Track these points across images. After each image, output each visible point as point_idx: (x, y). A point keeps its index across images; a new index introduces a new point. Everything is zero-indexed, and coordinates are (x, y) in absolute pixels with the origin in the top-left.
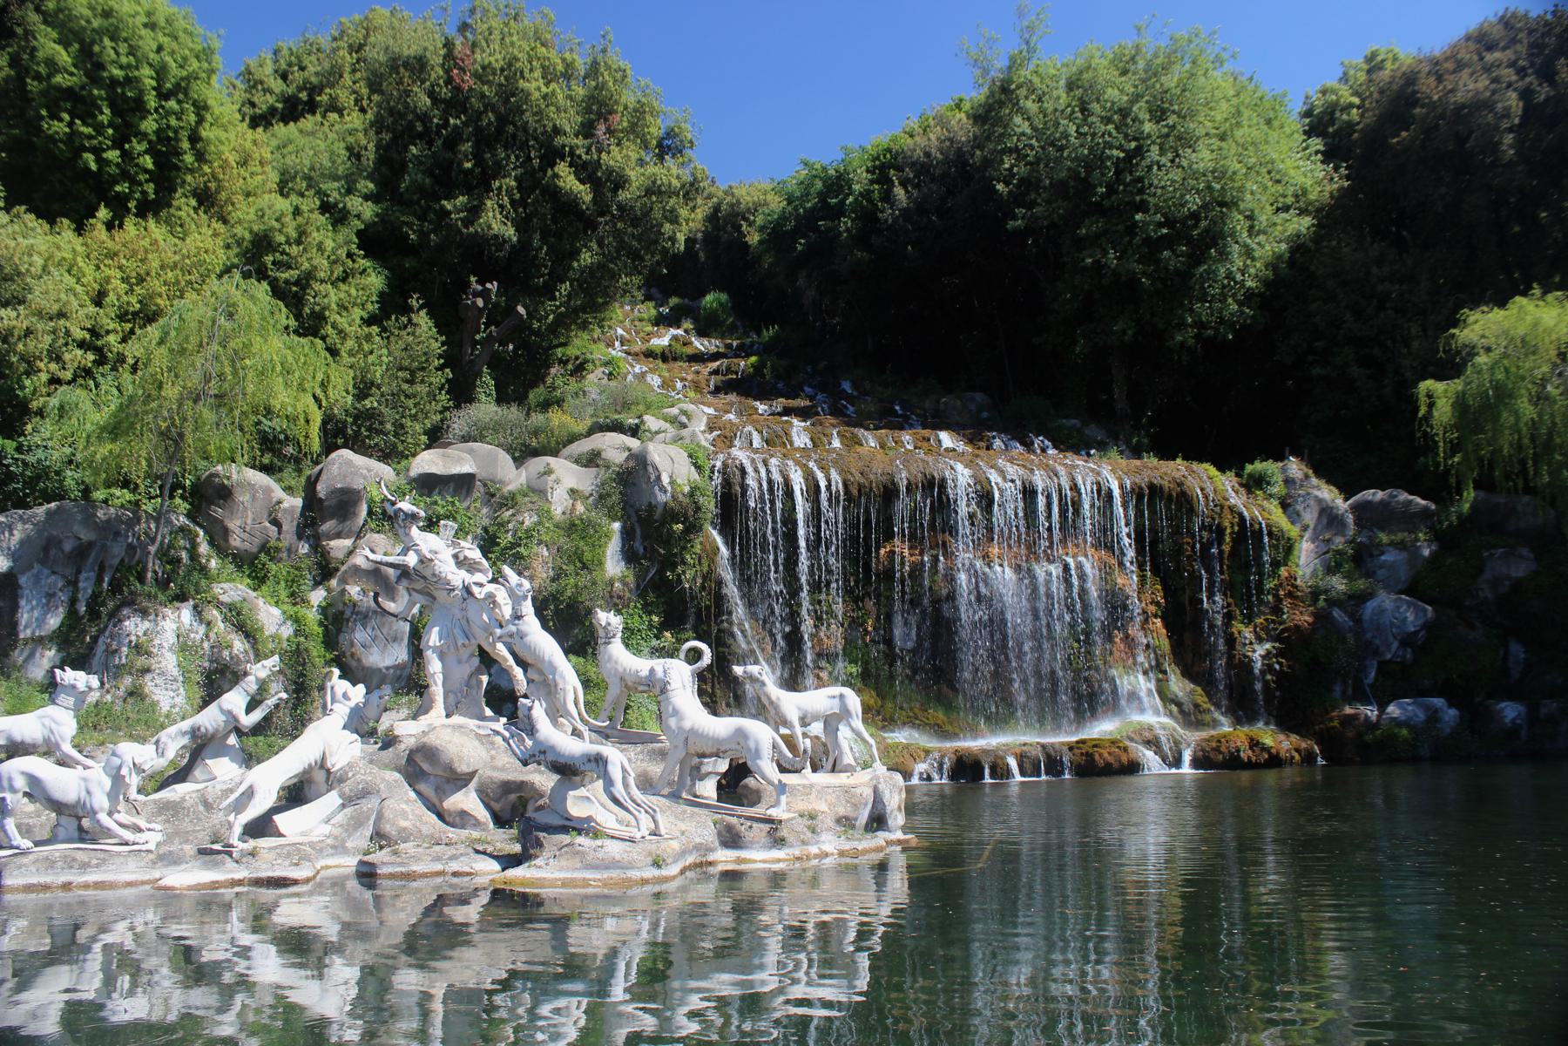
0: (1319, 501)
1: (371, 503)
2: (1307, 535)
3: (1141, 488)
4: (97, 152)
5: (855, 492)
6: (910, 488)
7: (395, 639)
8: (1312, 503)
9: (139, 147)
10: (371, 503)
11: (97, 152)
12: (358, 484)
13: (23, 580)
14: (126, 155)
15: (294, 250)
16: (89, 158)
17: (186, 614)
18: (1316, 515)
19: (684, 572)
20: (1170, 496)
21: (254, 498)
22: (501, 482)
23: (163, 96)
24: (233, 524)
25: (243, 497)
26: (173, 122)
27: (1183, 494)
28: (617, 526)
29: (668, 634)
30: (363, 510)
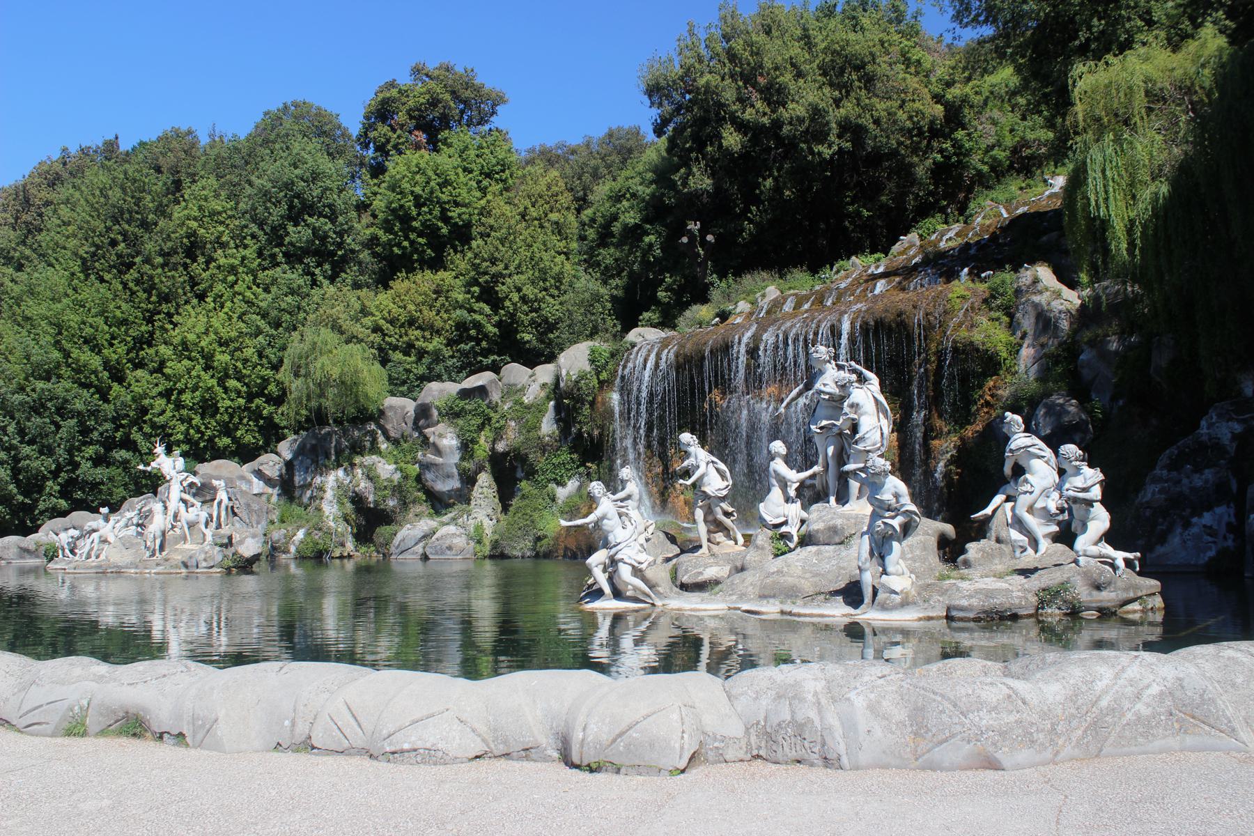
0: (1036, 306)
1: (438, 408)
2: (1027, 342)
3: (867, 324)
4: (399, 245)
5: (681, 360)
6: (711, 351)
7: (448, 477)
8: (1029, 309)
9: (413, 236)
10: (438, 408)
11: (399, 245)
12: (427, 401)
13: (296, 463)
14: (412, 243)
15: (485, 264)
16: (396, 250)
17: (340, 473)
18: (1033, 320)
19: (582, 428)
20: (890, 326)
21: (395, 413)
22: (515, 385)
23: (418, 205)
24: (389, 427)
25: (389, 414)
26: (429, 217)
27: (902, 322)
28: (552, 403)
29: (589, 464)
30: (435, 413)
